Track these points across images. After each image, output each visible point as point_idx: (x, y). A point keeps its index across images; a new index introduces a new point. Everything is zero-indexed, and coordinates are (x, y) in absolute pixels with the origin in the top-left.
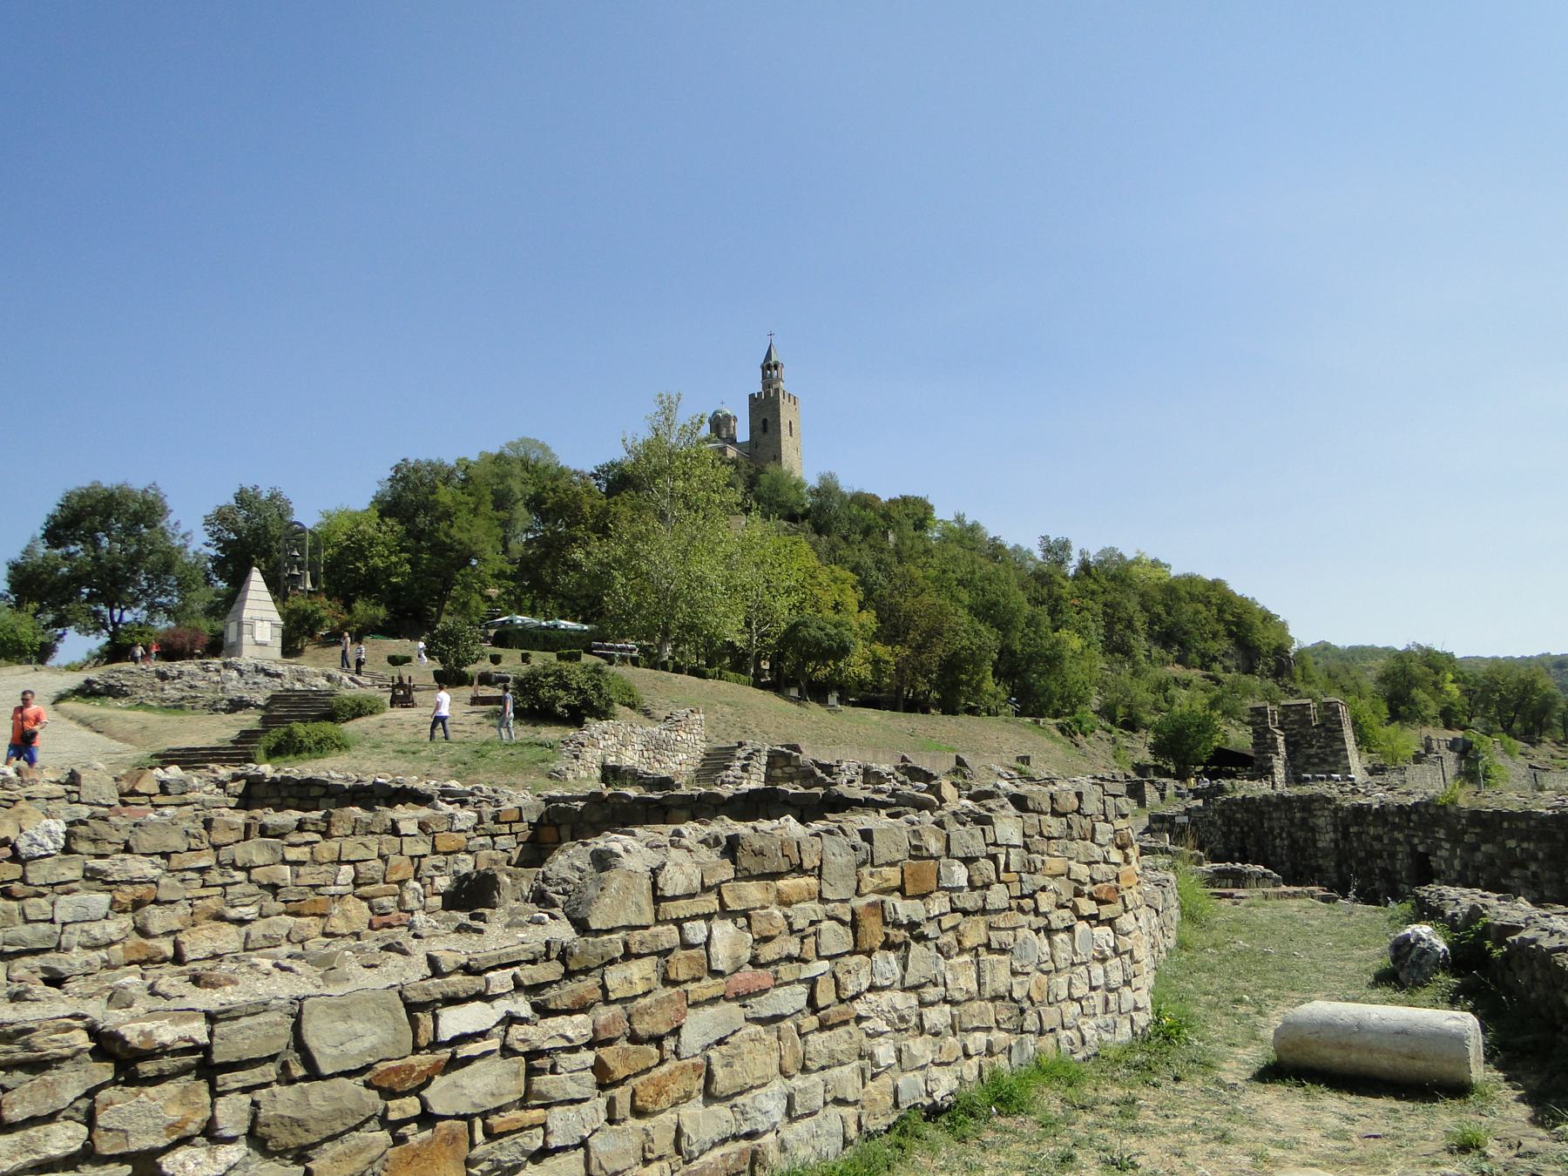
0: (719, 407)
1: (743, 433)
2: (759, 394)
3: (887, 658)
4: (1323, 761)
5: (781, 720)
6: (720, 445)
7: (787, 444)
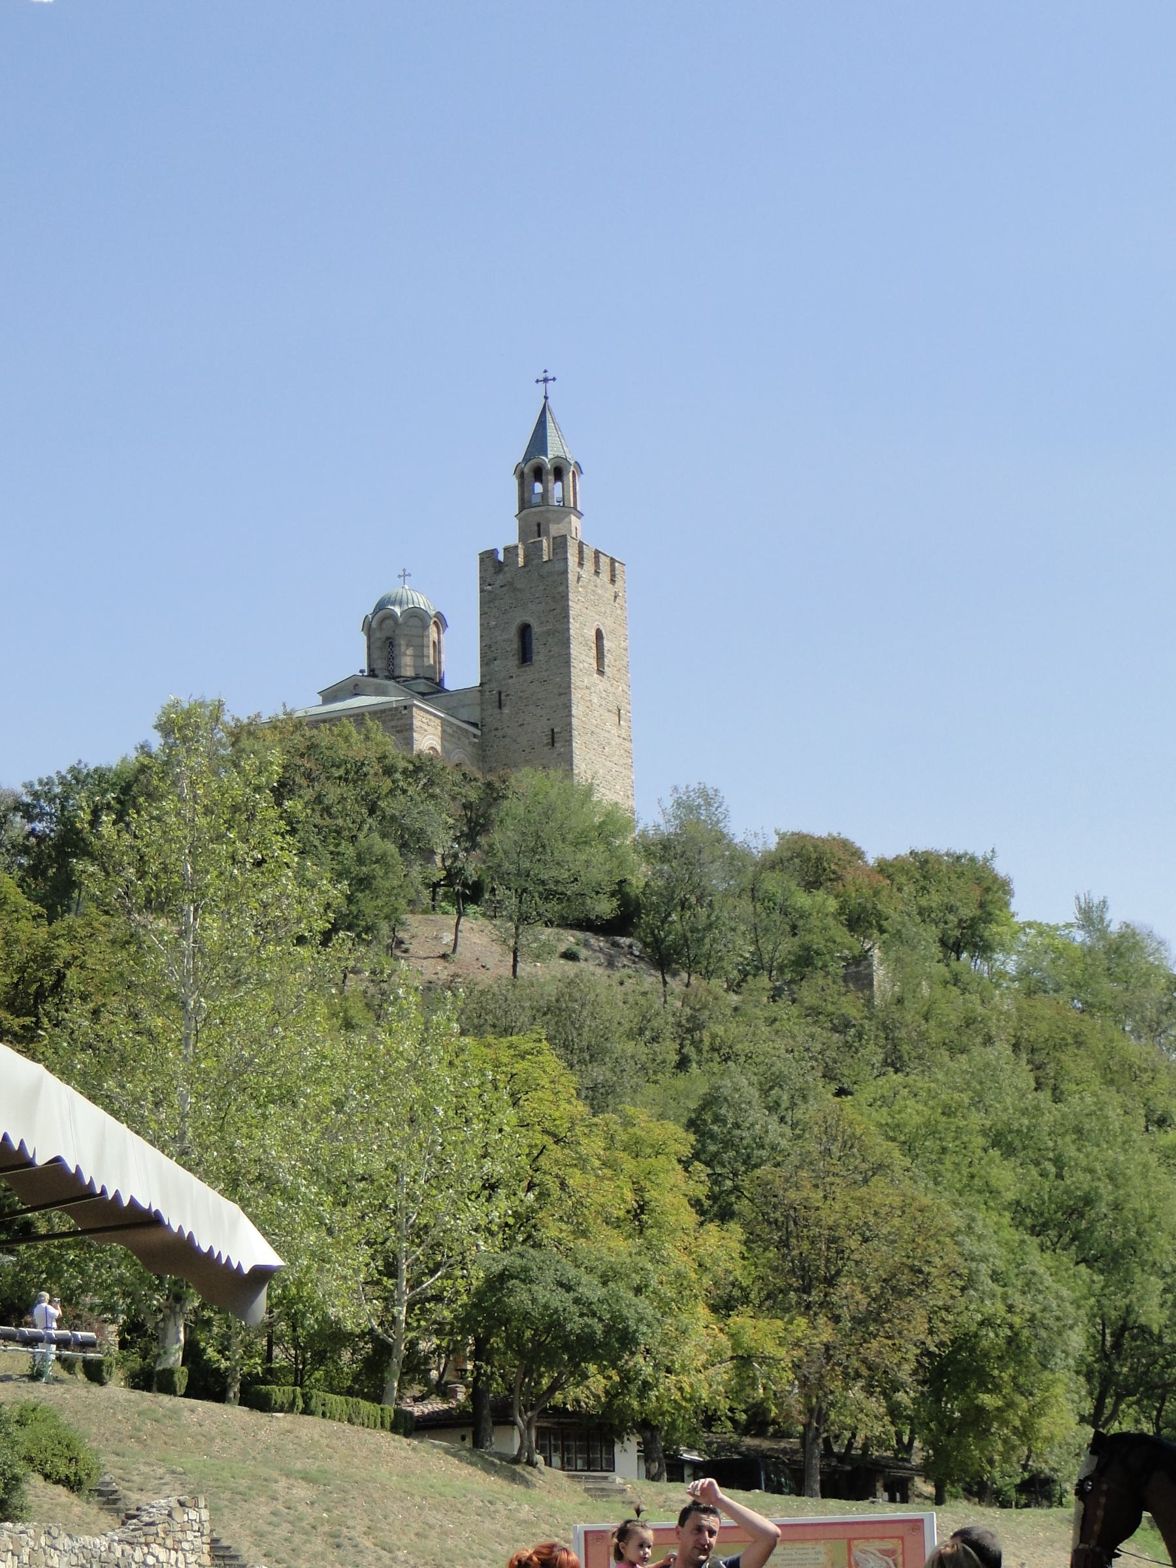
0: (394, 588)
3: (770, 1348)
5: (434, 1517)
6: (393, 699)
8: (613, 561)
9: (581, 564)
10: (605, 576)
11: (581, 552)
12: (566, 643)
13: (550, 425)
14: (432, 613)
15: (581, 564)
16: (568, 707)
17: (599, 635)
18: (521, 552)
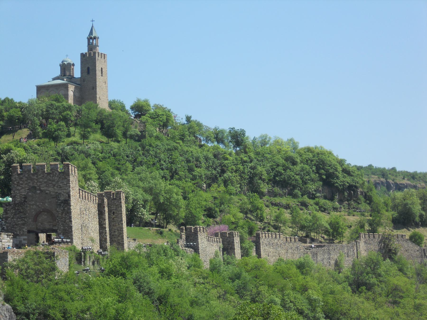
1: (77, 73)
2: (86, 54)
4: (194, 240)
6: (64, 82)
7: (99, 80)
8: (104, 54)
9: (98, 57)
10: (103, 58)
11: (98, 54)
12: (95, 71)
13: (93, 30)
14: (72, 63)
15: (98, 57)
16: (96, 82)
17: (102, 69)
18: (88, 54)
